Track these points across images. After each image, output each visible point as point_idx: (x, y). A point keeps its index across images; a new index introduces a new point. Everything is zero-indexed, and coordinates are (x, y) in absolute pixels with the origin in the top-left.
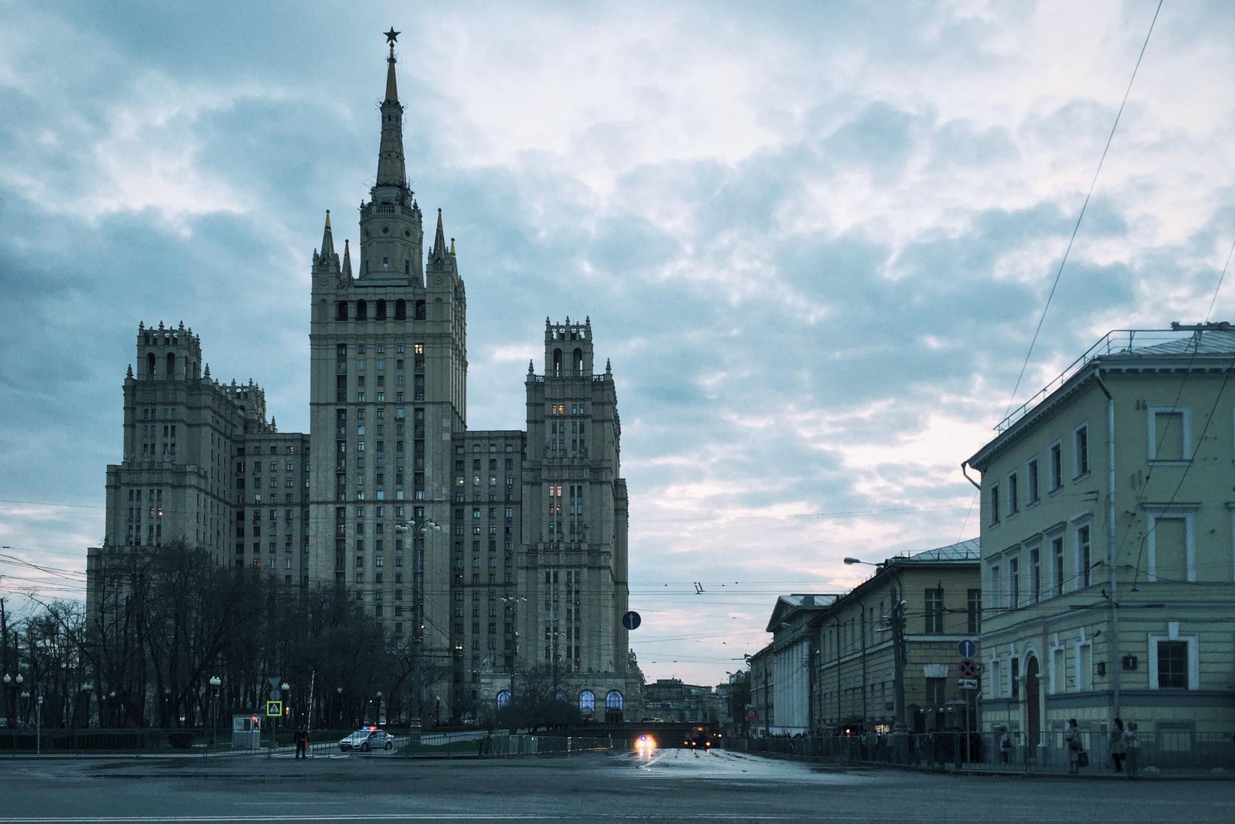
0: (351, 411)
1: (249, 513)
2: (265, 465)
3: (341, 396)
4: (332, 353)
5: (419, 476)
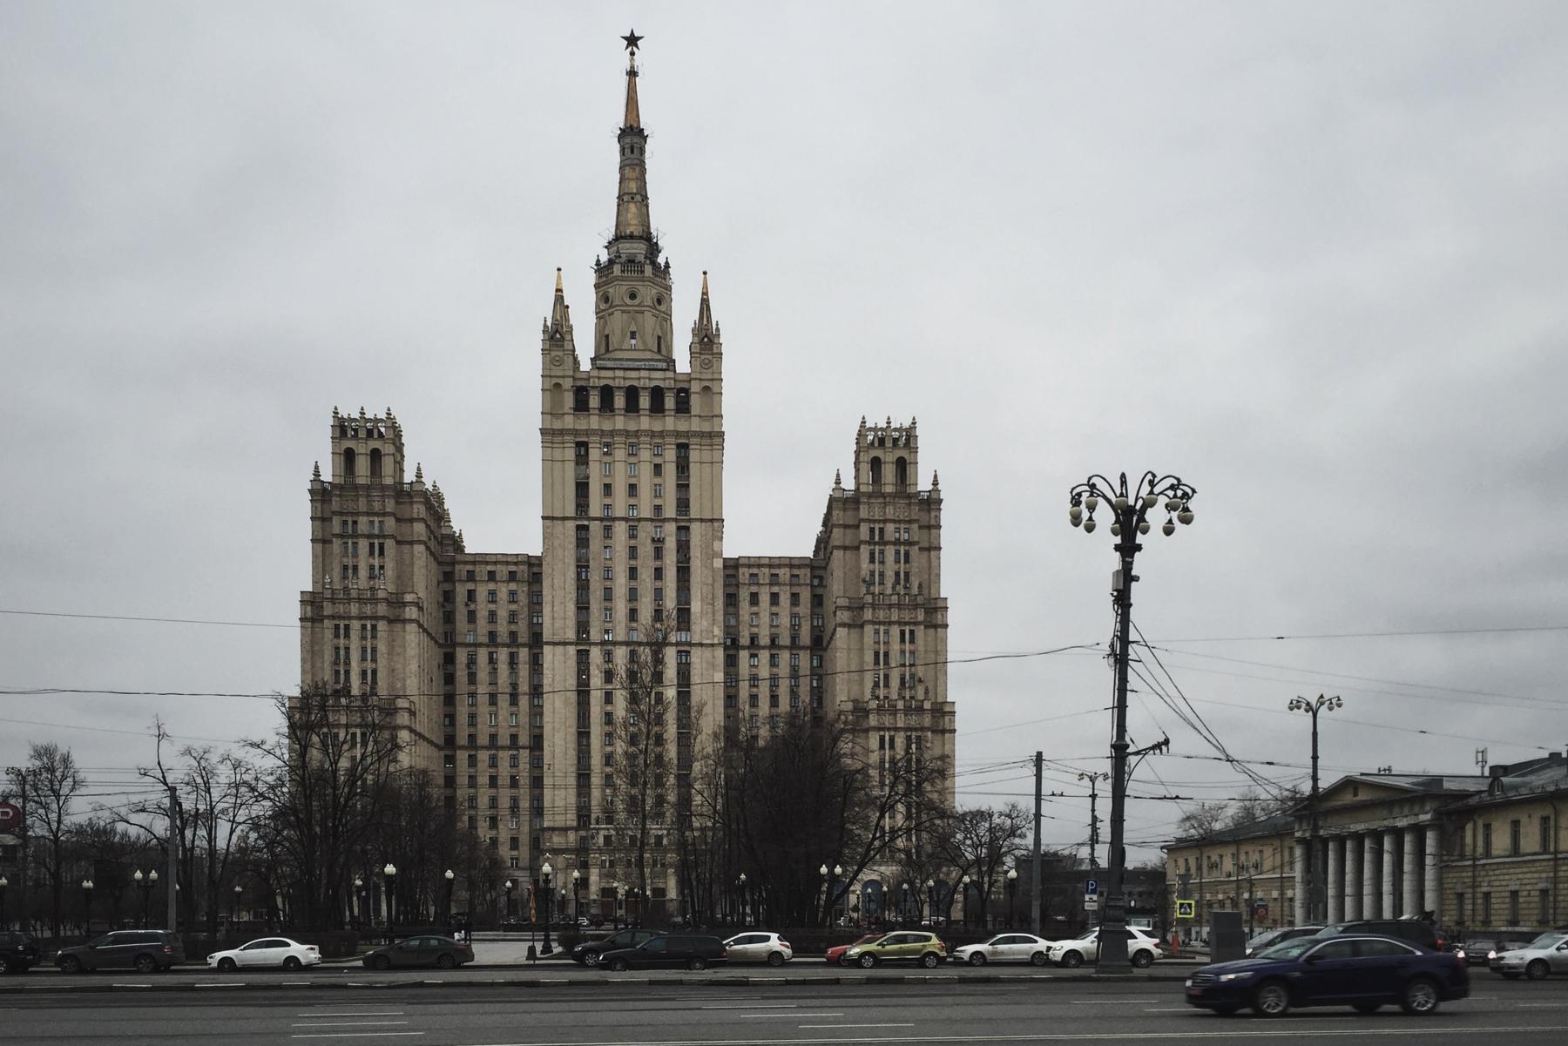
0: (596, 527)
1: (461, 656)
2: (482, 591)
4: (570, 453)
5: (684, 614)
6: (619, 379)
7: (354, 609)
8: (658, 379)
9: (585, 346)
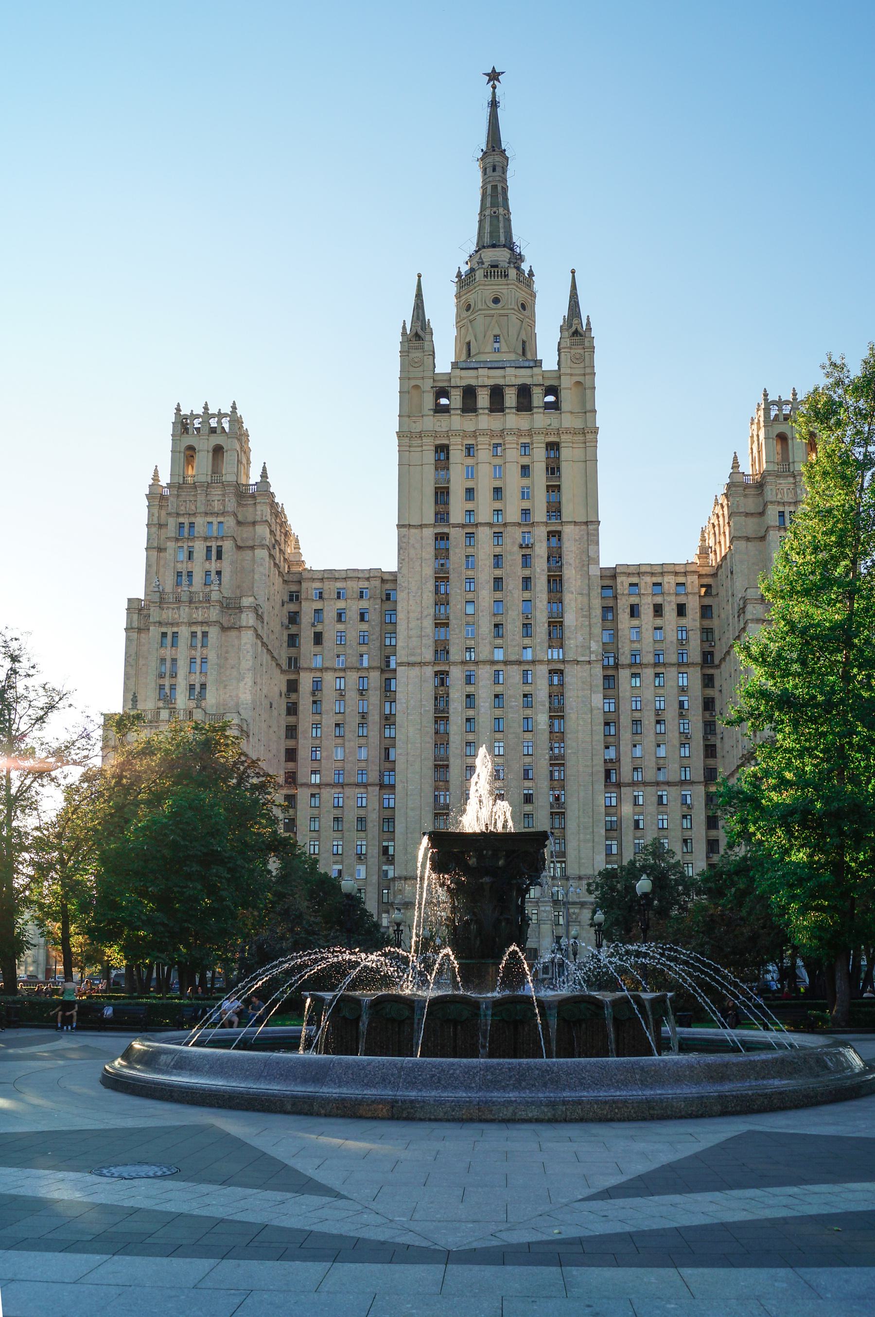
0: (457, 535)
3: (442, 516)
4: (430, 456)
5: (556, 625)
6: (486, 378)
7: (184, 613)
8: (523, 377)
9: (444, 359)
